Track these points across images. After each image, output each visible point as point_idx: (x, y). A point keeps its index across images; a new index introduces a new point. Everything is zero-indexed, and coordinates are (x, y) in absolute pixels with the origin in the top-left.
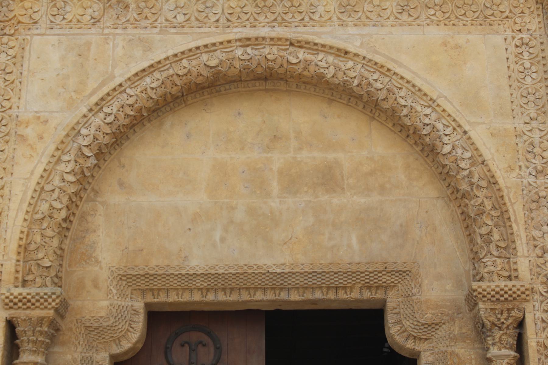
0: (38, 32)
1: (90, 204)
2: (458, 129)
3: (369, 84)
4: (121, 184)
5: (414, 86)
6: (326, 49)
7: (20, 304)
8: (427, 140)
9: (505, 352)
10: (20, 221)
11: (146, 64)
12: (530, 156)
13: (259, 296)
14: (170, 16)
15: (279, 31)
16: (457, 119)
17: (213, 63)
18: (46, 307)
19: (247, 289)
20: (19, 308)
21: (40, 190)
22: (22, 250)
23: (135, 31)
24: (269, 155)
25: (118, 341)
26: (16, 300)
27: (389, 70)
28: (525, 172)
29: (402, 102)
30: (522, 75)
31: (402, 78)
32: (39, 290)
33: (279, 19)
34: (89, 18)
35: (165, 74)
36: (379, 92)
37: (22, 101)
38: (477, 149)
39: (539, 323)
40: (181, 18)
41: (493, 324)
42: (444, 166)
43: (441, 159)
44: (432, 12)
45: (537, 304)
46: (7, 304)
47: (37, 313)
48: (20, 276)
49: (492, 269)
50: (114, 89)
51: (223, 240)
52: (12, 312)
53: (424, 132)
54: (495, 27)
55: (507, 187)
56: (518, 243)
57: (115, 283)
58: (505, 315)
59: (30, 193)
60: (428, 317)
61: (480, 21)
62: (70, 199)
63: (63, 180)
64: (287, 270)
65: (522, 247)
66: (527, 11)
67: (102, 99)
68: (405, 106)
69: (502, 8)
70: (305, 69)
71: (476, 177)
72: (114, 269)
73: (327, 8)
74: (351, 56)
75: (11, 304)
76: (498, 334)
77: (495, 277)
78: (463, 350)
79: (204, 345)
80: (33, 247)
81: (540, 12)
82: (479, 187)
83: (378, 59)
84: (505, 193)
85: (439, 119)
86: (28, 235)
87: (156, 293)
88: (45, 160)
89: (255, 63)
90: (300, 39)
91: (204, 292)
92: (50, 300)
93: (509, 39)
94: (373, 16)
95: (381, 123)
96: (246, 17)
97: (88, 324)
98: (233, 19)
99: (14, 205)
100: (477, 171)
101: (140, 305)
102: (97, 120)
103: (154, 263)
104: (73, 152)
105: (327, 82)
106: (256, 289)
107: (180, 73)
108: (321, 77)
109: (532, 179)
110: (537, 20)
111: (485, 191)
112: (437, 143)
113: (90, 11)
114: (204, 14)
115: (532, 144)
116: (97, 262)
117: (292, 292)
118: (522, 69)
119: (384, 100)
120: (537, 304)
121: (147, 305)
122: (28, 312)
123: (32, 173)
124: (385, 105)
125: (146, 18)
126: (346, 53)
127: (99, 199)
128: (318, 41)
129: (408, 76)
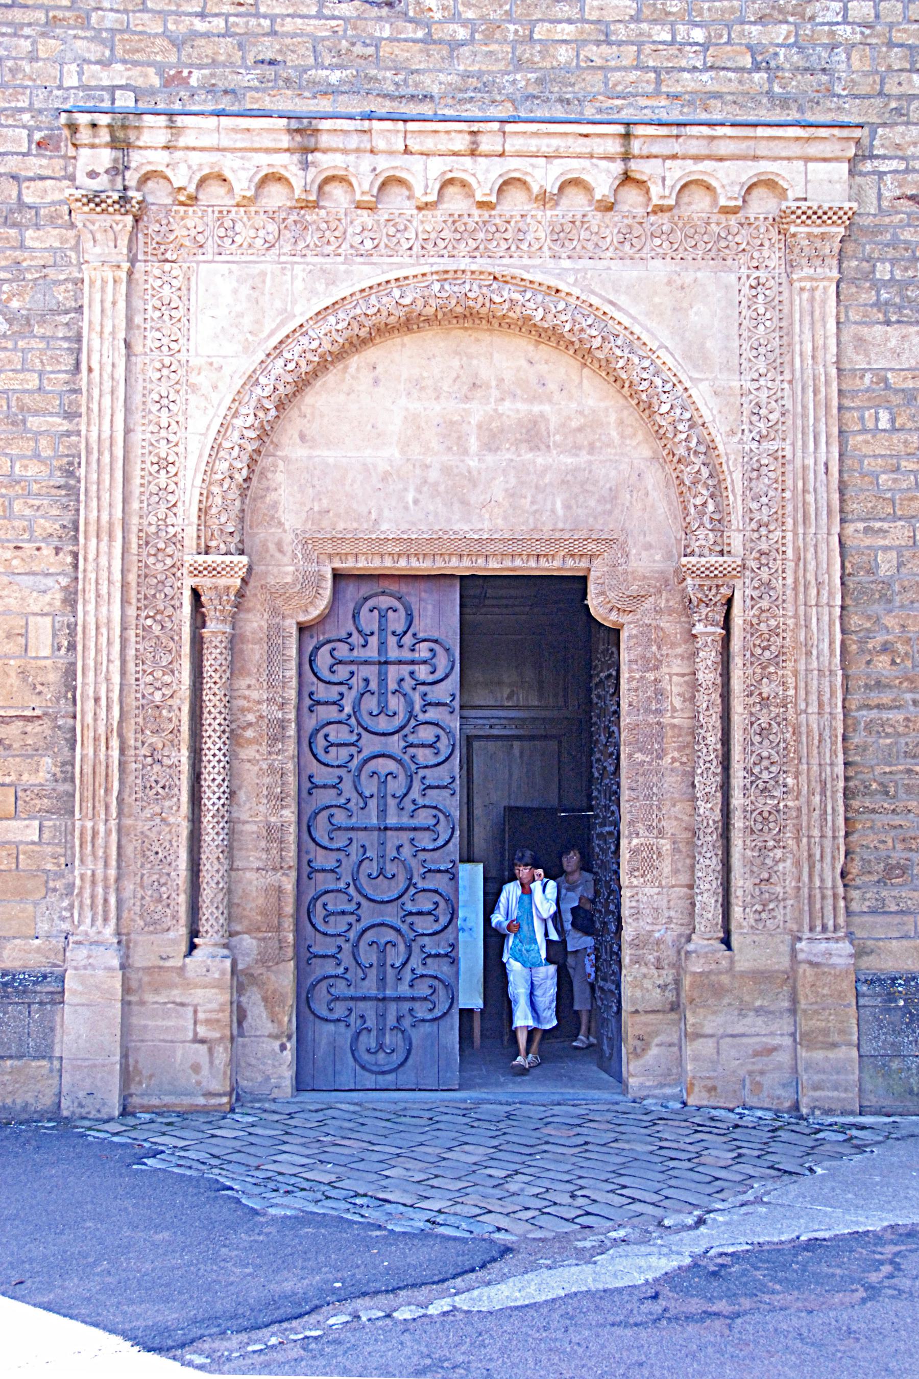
8: (644, 396)
9: (710, 629)
10: (198, 482)
11: (329, 302)
12: (755, 418)
21: (216, 448)
24: (467, 406)
29: (618, 352)
30: (754, 323)
40: (369, 244)
44: (657, 242)
45: (748, 581)
47: (222, 582)
51: (416, 502)
52: (197, 579)
54: (729, 262)
59: (207, 451)
65: (736, 519)
67: (281, 342)
73: (537, 235)
74: (563, 295)
76: (704, 611)
84: (723, 460)
93: (744, 278)
94: (590, 246)
96: (442, 244)
98: (429, 246)
104: (253, 403)
109: (754, 445)
113: (262, 233)
114: (395, 240)
115: (758, 405)
118: (754, 315)
120: (748, 581)
124: (600, 355)
128: (525, 276)
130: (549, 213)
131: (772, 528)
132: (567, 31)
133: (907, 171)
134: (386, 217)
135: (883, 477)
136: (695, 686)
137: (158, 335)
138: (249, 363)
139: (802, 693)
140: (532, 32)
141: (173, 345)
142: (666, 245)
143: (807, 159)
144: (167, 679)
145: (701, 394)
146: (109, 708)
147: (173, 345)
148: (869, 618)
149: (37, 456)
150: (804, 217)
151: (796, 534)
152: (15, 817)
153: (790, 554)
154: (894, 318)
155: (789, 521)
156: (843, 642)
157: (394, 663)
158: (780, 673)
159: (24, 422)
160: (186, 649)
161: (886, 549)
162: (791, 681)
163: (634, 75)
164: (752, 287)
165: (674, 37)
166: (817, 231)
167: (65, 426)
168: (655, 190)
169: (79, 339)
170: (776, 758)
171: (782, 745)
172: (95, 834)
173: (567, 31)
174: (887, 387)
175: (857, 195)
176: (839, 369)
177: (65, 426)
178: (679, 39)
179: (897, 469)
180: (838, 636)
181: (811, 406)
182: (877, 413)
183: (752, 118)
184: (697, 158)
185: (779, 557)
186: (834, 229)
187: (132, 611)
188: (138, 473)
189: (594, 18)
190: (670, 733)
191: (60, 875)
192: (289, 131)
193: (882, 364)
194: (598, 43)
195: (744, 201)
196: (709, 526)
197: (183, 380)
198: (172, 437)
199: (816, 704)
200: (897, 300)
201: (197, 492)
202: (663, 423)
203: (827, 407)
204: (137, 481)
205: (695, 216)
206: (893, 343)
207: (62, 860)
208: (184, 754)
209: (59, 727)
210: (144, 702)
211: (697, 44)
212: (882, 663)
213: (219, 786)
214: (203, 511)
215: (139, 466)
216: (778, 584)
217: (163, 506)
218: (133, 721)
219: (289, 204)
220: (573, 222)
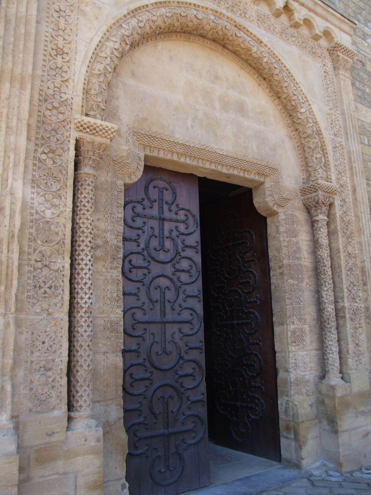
2: (306, 102)
5: (289, 73)
6: (252, 36)
7: (88, 130)
16: (307, 97)
18: (106, 137)
20: (87, 132)
21: (95, 54)
26: (86, 126)
36: (275, 70)
46: (78, 127)
51: (192, 127)
58: (328, 199)
59: (90, 54)
68: (286, 82)
72: (130, 127)
75: (81, 128)
78: (299, 215)
87: (152, 149)
90: (241, 24)
91: (180, 155)
92: (110, 132)
95: (263, 89)
97: (115, 159)
102: (134, 22)
103: (154, 129)
112: (298, 106)
117: (224, 167)
119: (276, 75)
122: (92, 137)
123: (92, 40)
127: (119, 78)
130: (256, 7)
187: (32, 147)
198: (67, 37)
201: (83, 77)
210: (35, 216)
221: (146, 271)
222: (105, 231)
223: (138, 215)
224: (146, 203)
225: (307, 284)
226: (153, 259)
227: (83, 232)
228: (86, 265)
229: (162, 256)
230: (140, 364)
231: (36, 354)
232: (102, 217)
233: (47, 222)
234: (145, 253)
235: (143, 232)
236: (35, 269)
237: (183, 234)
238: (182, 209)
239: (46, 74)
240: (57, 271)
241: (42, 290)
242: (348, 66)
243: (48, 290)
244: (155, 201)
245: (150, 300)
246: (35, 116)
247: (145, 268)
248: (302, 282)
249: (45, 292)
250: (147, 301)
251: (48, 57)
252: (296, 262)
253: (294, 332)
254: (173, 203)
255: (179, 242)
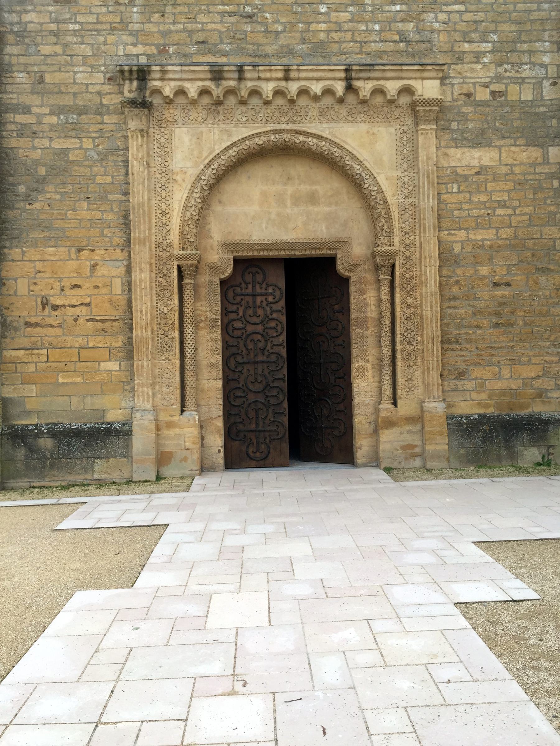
0: (177, 126)
1: (207, 211)
3: (332, 154)
4: (220, 202)
5: (353, 154)
6: (313, 135)
8: (358, 181)
10: (178, 221)
11: (229, 143)
12: (402, 189)
13: (282, 253)
14: (239, 117)
15: (291, 126)
17: (260, 143)
19: (277, 250)
21: (186, 206)
22: (181, 234)
23: (224, 126)
24: (286, 187)
25: (223, 273)
27: (341, 146)
28: (400, 197)
29: (347, 163)
31: (347, 150)
32: (190, 252)
33: (291, 119)
34: (201, 118)
35: (238, 149)
37: (174, 162)
38: (380, 186)
39: (401, 264)
40: (244, 119)
41: (382, 266)
42: (365, 194)
43: (363, 190)
44: (363, 115)
45: (401, 257)
47: (190, 262)
48: (181, 245)
49: (383, 241)
50: (215, 157)
51: (266, 228)
52: (179, 261)
53: (357, 177)
54: (392, 123)
55: (392, 204)
56: (395, 230)
57: (220, 247)
58: (387, 262)
59: (182, 208)
60: (355, 262)
61: (385, 120)
62: (199, 210)
63: (196, 201)
64: (295, 241)
65: (396, 231)
66: (407, 115)
67: (210, 161)
69: (395, 113)
70: (303, 145)
71: (379, 199)
74: (324, 139)
76: (384, 270)
77: (384, 246)
79: (259, 273)
80: (185, 233)
81: (413, 115)
82: (380, 204)
83: (337, 140)
84: (391, 206)
85: (363, 171)
86: (182, 227)
88: (187, 192)
89: (280, 143)
94: (335, 118)
96: (275, 118)
99: (175, 213)
100: (379, 196)
101: (231, 257)
102: (208, 172)
103: (236, 238)
104: (199, 188)
105: (313, 153)
106: (281, 250)
107: (245, 148)
108: (310, 149)
109: (403, 200)
110: (412, 119)
111: (382, 206)
112: (362, 183)
113: (201, 114)
115: (404, 183)
116: (212, 238)
121: (234, 257)
122: (186, 262)
123: (182, 198)
124: (340, 164)
125: (228, 119)
126: (322, 137)
128: (309, 131)
129: (350, 149)
130: (318, 104)
131: (410, 234)
132: (323, 26)
133: (463, 83)
134: (251, 107)
135: (455, 212)
136: (380, 301)
137: (160, 159)
138: (197, 171)
139: (424, 302)
140: (309, 27)
141: (166, 163)
142: (366, 116)
143: (423, 79)
144: (169, 303)
145: (381, 179)
146: (146, 315)
147: (166, 163)
148: (450, 271)
149: (112, 210)
150: (422, 103)
151: (420, 237)
152: (110, 360)
153: (418, 245)
154: (459, 145)
155: (417, 232)
156: (440, 281)
157: (259, 295)
158: (414, 294)
159: (106, 197)
160: (176, 291)
161: (456, 242)
162: (419, 297)
163: (351, 44)
164: (401, 134)
165: (367, 28)
166: (427, 109)
167: (124, 198)
168: (361, 94)
169: (127, 161)
170: (413, 329)
171: (416, 324)
172: (142, 366)
173: (323, 26)
174: (457, 174)
175: (443, 93)
176: (437, 167)
177: (124, 198)
178: (369, 29)
179: (460, 209)
180: (438, 279)
181: (426, 183)
182: (452, 186)
183: (400, 62)
184: (378, 79)
185: (414, 247)
186: (434, 108)
187: (154, 275)
188: (154, 217)
189: (334, 20)
190: (370, 320)
191: (128, 383)
192: (211, 71)
193: (453, 164)
194: (336, 31)
195: (397, 97)
196: (385, 235)
197: (171, 178)
198: (167, 202)
199: (429, 306)
200: (460, 138)
201: (178, 225)
202: (366, 192)
203: (433, 184)
204: (154, 221)
205: (377, 104)
206: (459, 156)
207: (129, 377)
208: (177, 334)
209: (126, 323)
210: (159, 312)
211: (376, 31)
212: (455, 289)
213: (191, 346)
214: (182, 233)
215: (154, 214)
216: (413, 258)
217: (165, 231)
218: (156, 320)
219: (211, 102)
220: (328, 108)
221: (244, 331)
222: (206, 312)
223: (238, 295)
224: (243, 285)
225: (372, 331)
226: (248, 322)
227: (186, 316)
228: (189, 333)
229: (255, 320)
230: (240, 388)
231: (164, 379)
232: (203, 303)
233: (166, 314)
234: (243, 319)
235: (241, 306)
236: (161, 339)
237: (271, 303)
238: (271, 285)
239: (157, 230)
240: (172, 338)
241: (165, 349)
242: (433, 116)
243: (168, 348)
244: (250, 283)
245: (247, 349)
246: (154, 258)
247: (243, 329)
248: (366, 330)
249: (167, 350)
250: (244, 349)
251: (158, 219)
252: (363, 315)
253: (358, 369)
254: (263, 282)
255: (268, 309)
